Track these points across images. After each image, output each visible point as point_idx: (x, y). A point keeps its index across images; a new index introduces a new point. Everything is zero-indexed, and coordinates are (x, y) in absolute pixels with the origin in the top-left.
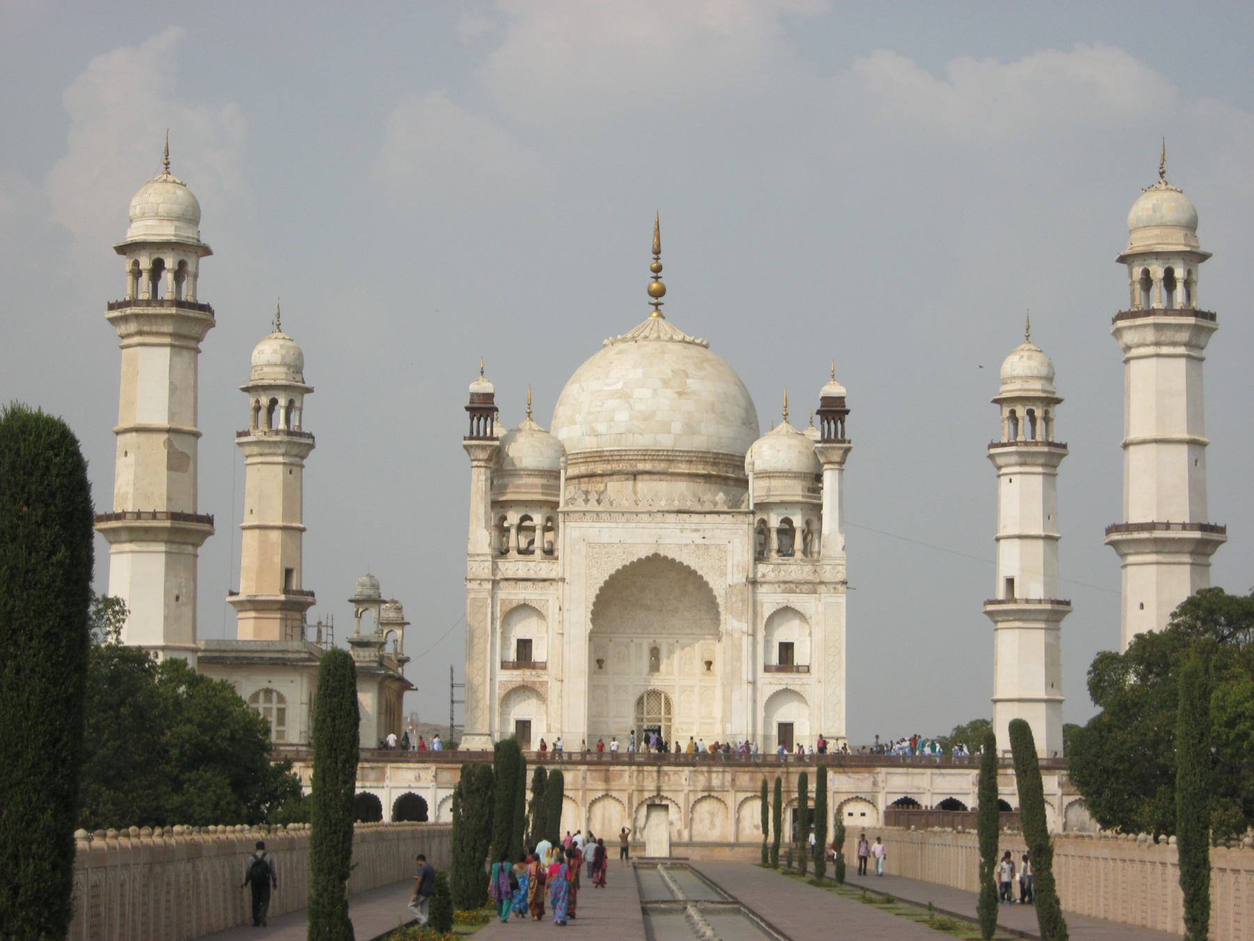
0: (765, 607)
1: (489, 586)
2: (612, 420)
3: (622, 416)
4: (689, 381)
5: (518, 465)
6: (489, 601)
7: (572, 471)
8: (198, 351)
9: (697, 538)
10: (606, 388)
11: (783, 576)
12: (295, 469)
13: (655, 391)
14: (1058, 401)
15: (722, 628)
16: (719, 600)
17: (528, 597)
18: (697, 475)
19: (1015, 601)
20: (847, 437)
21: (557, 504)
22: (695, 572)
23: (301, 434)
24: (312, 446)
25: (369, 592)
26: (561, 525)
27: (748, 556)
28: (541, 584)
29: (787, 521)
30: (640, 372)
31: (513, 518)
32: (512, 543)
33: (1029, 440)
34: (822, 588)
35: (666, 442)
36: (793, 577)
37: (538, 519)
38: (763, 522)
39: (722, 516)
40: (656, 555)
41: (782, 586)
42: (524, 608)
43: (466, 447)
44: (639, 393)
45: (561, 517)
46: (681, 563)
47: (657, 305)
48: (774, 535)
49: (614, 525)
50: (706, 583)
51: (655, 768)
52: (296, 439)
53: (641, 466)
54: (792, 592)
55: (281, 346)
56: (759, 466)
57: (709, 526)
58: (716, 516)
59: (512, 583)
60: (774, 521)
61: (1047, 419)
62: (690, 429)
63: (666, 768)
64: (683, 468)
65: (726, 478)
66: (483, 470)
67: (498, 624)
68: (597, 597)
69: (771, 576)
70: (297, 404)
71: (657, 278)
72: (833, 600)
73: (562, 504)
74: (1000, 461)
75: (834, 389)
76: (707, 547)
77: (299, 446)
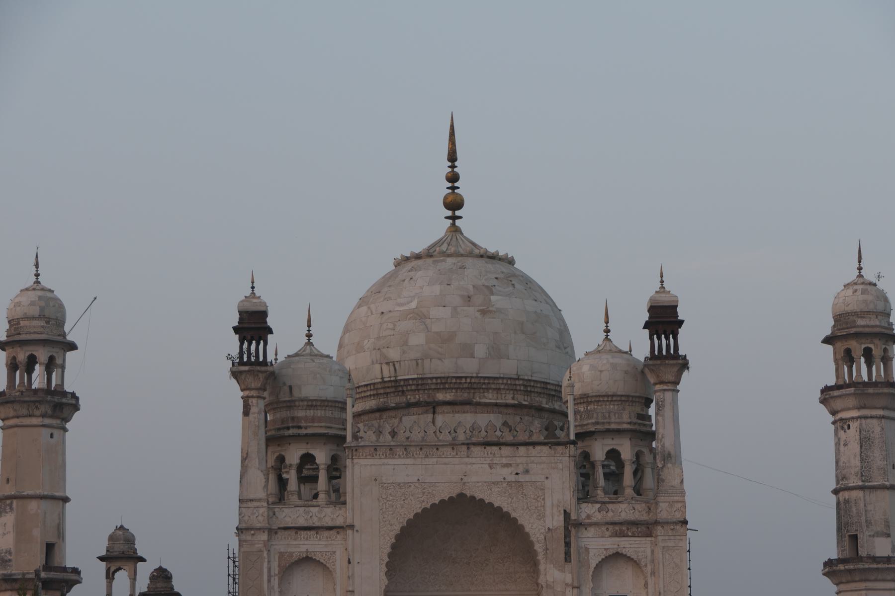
0: (591, 554)
1: (264, 537)
2: (406, 343)
3: (417, 340)
4: (493, 298)
5: (296, 394)
6: (265, 555)
7: (360, 407)
9: (507, 473)
10: (398, 308)
12: (56, 433)
13: (455, 308)
15: (542, 580)
16: (538, 547)
18: (507, 406)
19: (860, 559)
20: (681, 352)
21: (343, 438)
22: (507, 514)
23: (64, 394)
24: (76, 408)
25: (120, 547)
26: (349, 462)
28: (326, 533)
29: (613, 454)
30: (437, 289)
31: (294, 455)
32: (293, 485)
33: (865, 378)
34: (659, 530)
35: (469, 367)
37: (322, 457)
38: (586, 456)
39: (538, 448)
40: (461, 495)
41: (611, 528)
42: (307, 560)
43: (235, 374)
44: (436, 312)
46: (491, 504)
47: (454, 218)
48: (600, 472)
50: (521, 527)
52: (56, 399)
53: (440, 396)
54: (622, 535)
55: (40, 298)
56: (578, 390)
57: (524, 460)
58: (531, 447)
59: (293, 532)
61: (886, 360)
62: (497, 352)
64: (490, 398)
65: (540, 409)
67: (275, 582)
68: (393, 547)
69: (598, 517)
70: (59, 361)
71: (453, 188)
72: (671, 544)
73: (349, 438)
74: (838, 404)
75: (664, 300)
76: (520, 485)
77: (61, 406)
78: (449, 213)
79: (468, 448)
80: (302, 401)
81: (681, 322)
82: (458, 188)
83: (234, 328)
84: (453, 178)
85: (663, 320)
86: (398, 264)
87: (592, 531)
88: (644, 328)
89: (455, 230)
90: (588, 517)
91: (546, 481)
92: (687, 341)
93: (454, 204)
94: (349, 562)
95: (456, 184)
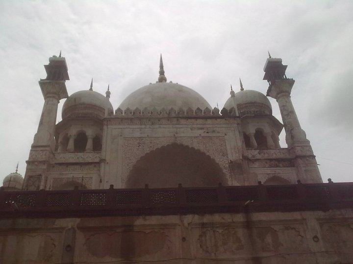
1: (45, 167)
11: (266, 156)
16: (224, 171)
17: (75, 176)
27: (240, 143)
31: (73, 131)
36: (274, 156)
37: (90, 132)
39: (219, 120)
45: (105, 123)
49: (143, 126)
51: (239, 218)
57: (211, 126)
60: (251, 130)
63: (260, 217)
66: (51, 99)
69: (259, 157)
79: (178, 120)
80: (81, 104)
83: (46, 66)
85: (275, 71)
87: (257, 165)
90: (254, 156)
91: (226, 137)
94: (101, 182)
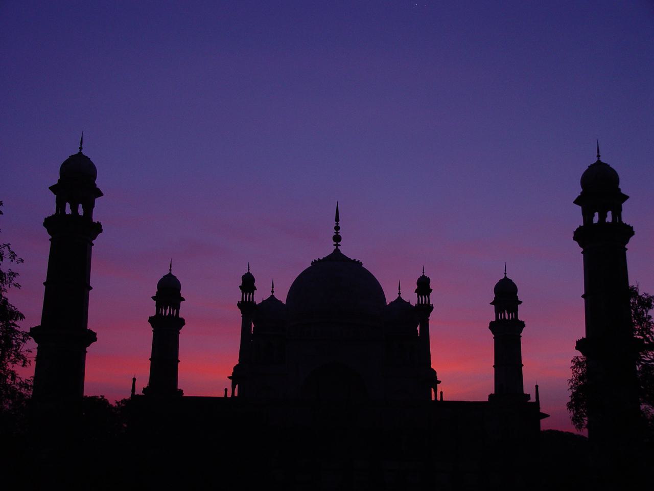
8: (93, 245)
14: (520, 302)
20: (431, 304)
47: (337, 245)
71: (337, 233)
78: (335, 243)
81: (432, 290)
82: (339, 233)
84: (337, 228)
86: (312, 263)
88: (415, 292)
89: (337, 251)
92: (434, 298)
93: (337, 238)
95: (338, 231)
